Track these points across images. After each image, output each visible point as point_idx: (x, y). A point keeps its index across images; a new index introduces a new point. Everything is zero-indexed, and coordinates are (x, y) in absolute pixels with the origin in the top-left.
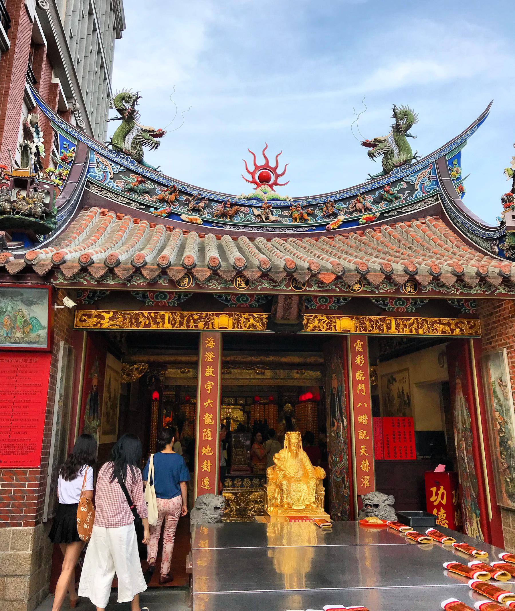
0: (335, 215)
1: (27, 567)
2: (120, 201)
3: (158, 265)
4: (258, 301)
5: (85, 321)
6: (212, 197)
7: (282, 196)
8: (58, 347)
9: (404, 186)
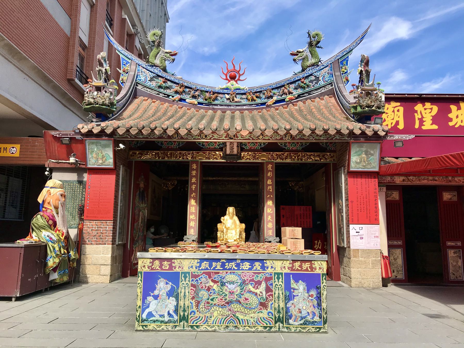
0: (271, 97)
1: (109, 262)
2: (154, 93)
3: (162, 128)
4: (219, 146)
5: (133, 156)
6: (203, 89)
7: (242, 87)
8: (120, 167)
9: (313, 78)
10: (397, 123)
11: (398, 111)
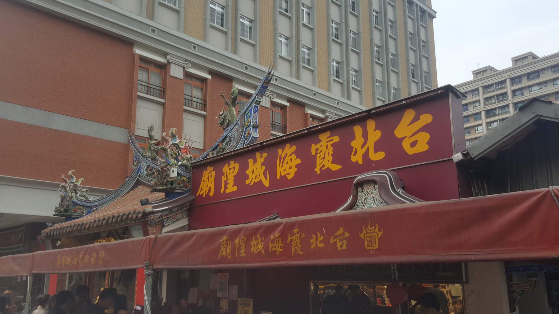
9: (227, 140)
11: (211, 176)
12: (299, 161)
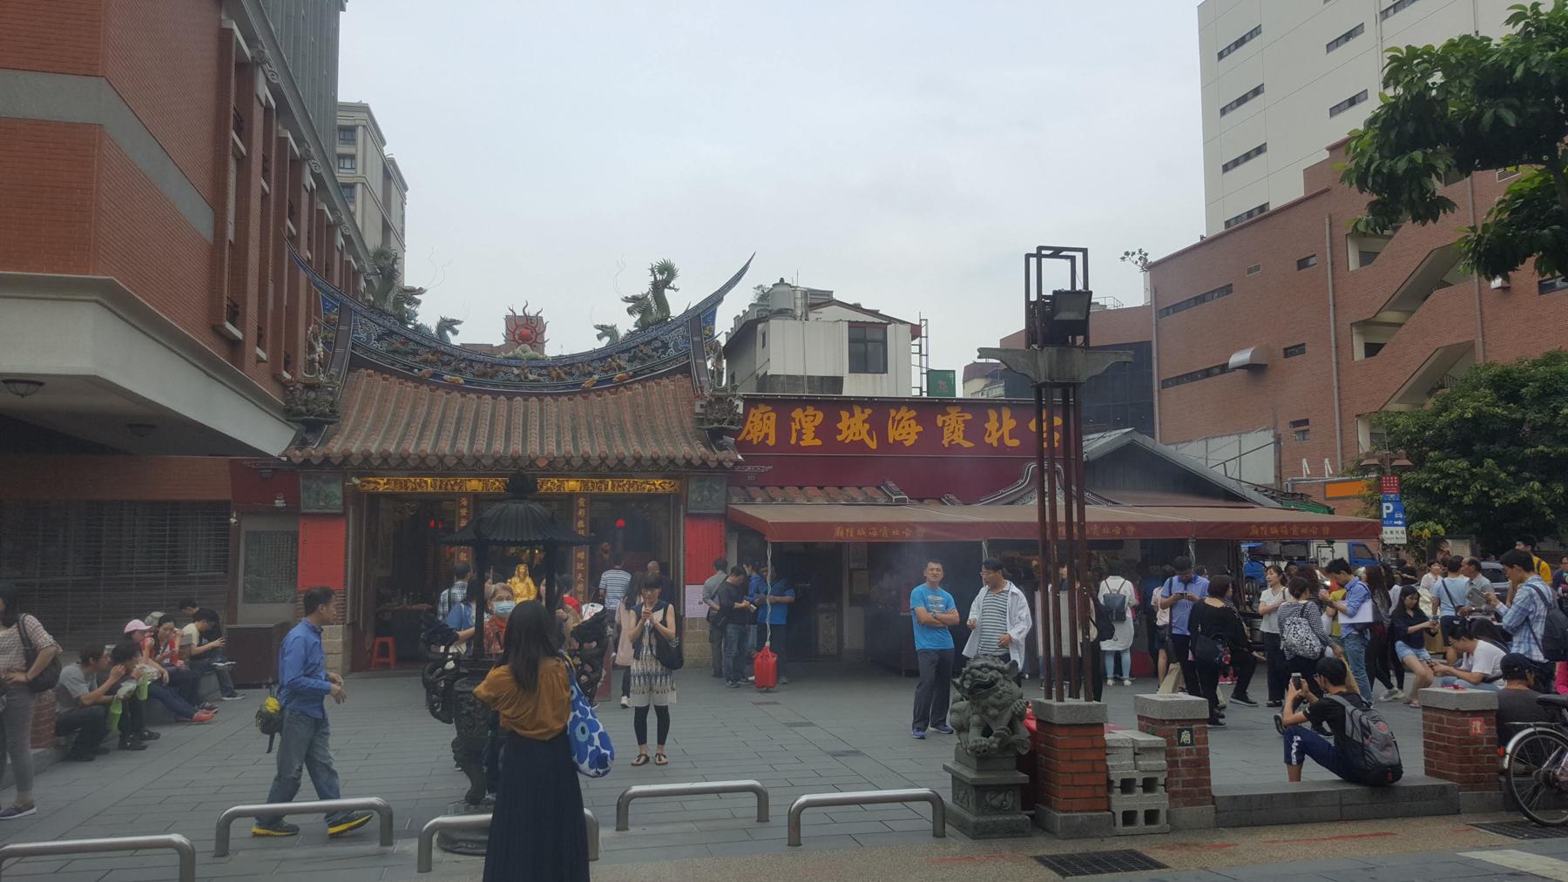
0: (591, 374)
1: (340, 649)
10: (766, 436)
12: (920, 429)
